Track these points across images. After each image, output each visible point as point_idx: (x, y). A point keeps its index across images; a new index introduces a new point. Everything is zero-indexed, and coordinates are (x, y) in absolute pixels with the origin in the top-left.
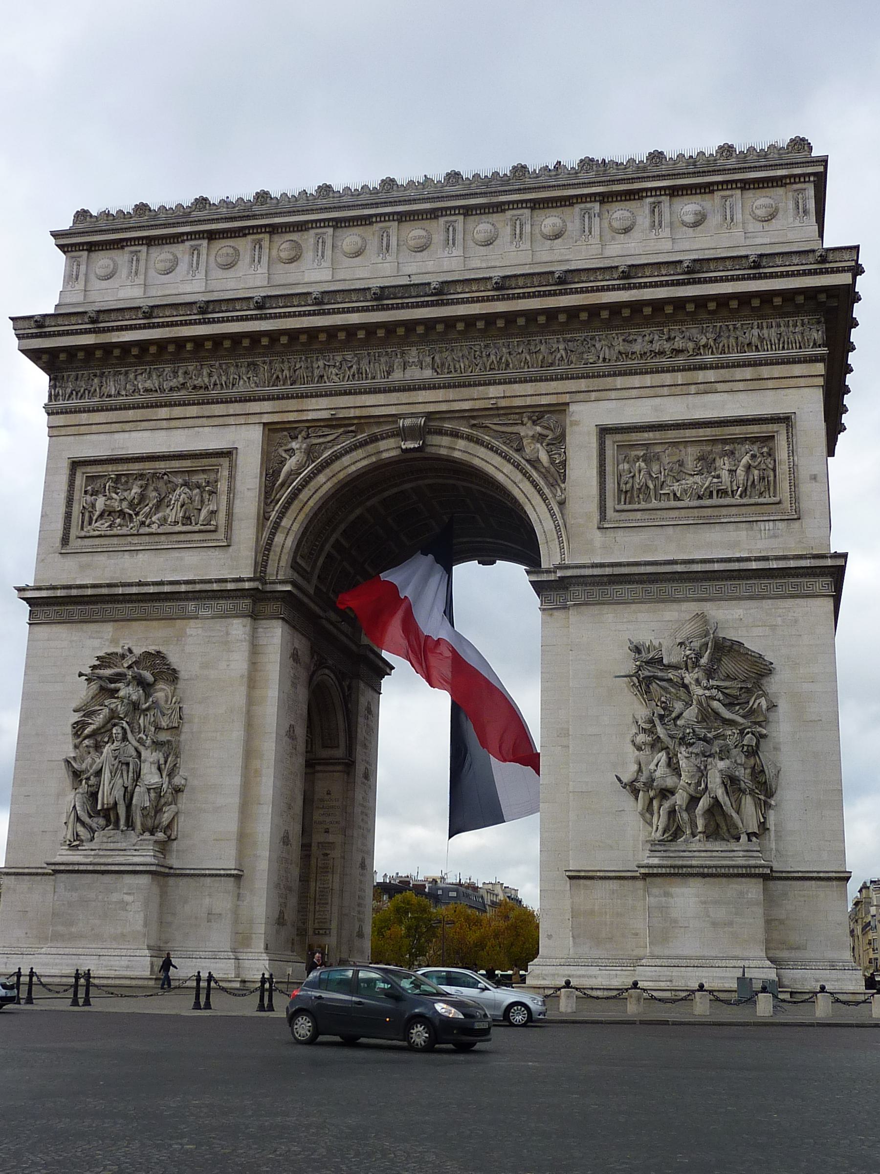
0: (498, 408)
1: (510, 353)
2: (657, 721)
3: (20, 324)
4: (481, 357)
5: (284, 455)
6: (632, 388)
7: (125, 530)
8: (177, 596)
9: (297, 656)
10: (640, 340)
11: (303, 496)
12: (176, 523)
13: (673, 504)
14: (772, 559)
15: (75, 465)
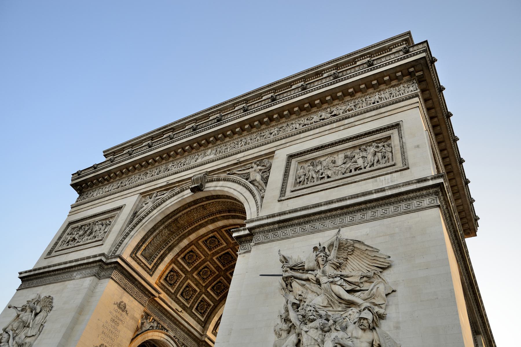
0: (240, 162)
1: (251, 139)
2: (290, 306)
3: (75, 175)
4: (238, 144)
5: (144, 205)
6: (309, 136)
7: (71, 246)
8: (71, 269)
9: (125, 307)
10: (315, 117)
11: (144, 221)
12: (90, 239)
13: (326, 180)
14: (387, 190)
15: (70, 224)
